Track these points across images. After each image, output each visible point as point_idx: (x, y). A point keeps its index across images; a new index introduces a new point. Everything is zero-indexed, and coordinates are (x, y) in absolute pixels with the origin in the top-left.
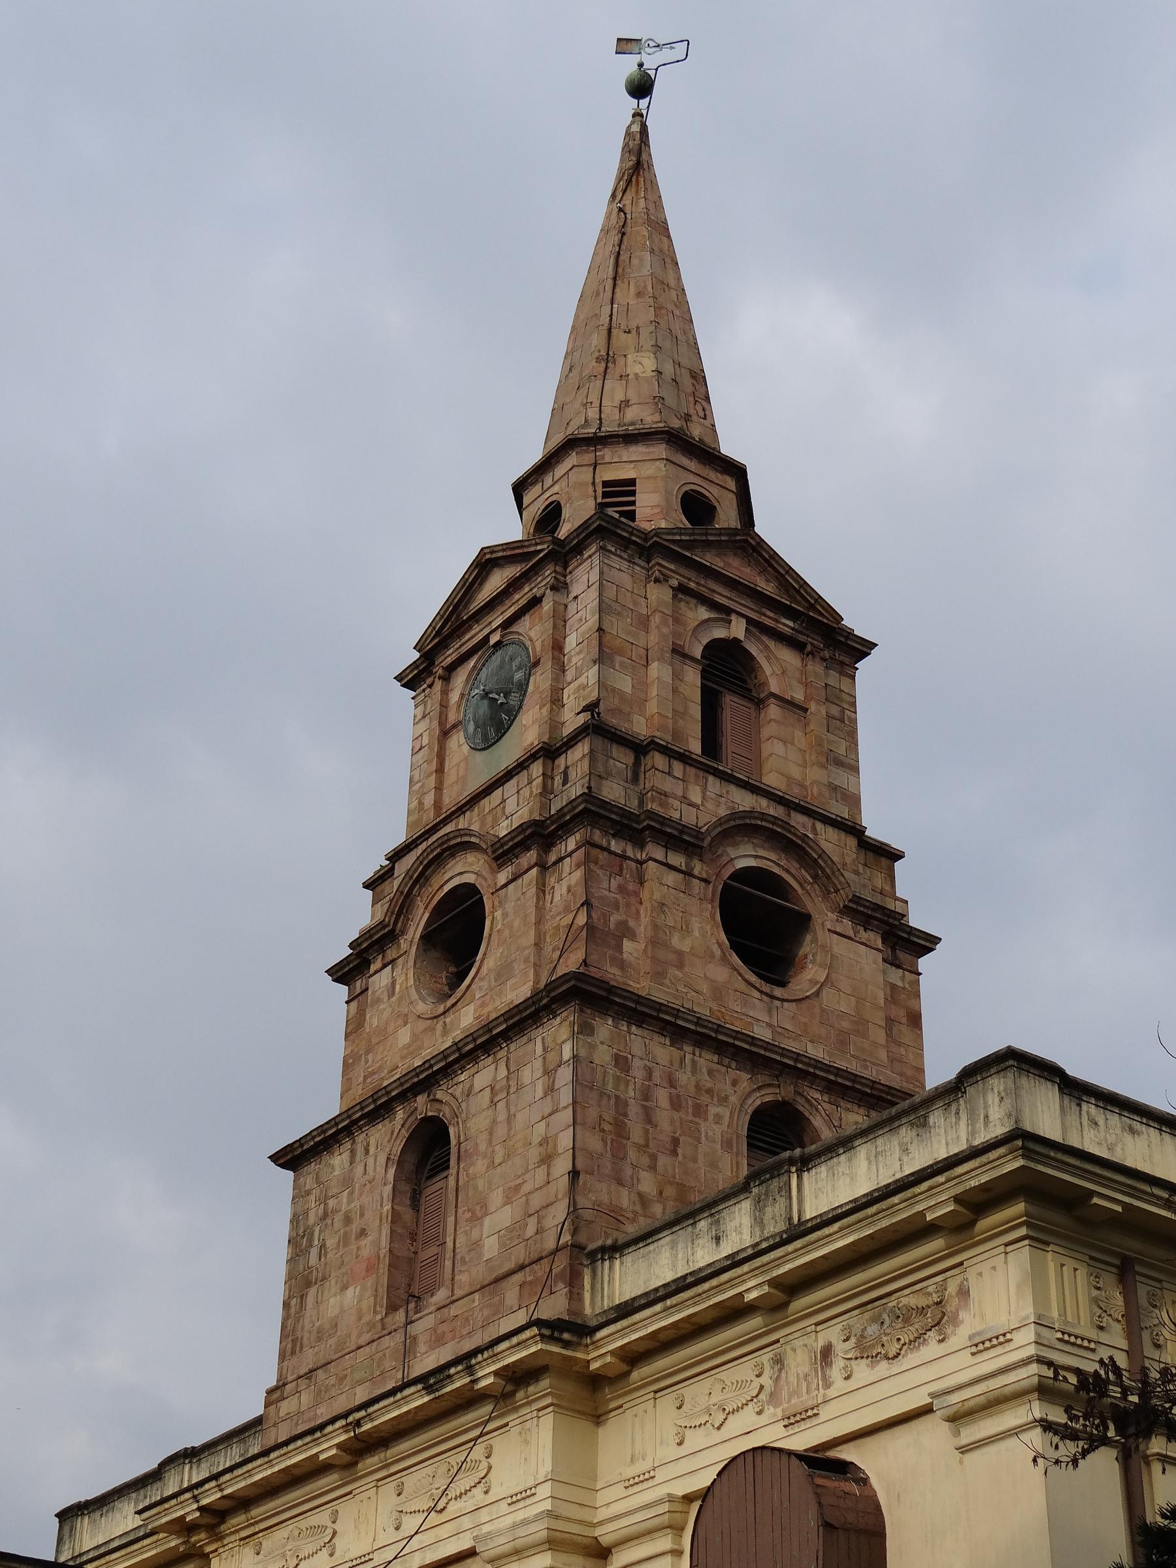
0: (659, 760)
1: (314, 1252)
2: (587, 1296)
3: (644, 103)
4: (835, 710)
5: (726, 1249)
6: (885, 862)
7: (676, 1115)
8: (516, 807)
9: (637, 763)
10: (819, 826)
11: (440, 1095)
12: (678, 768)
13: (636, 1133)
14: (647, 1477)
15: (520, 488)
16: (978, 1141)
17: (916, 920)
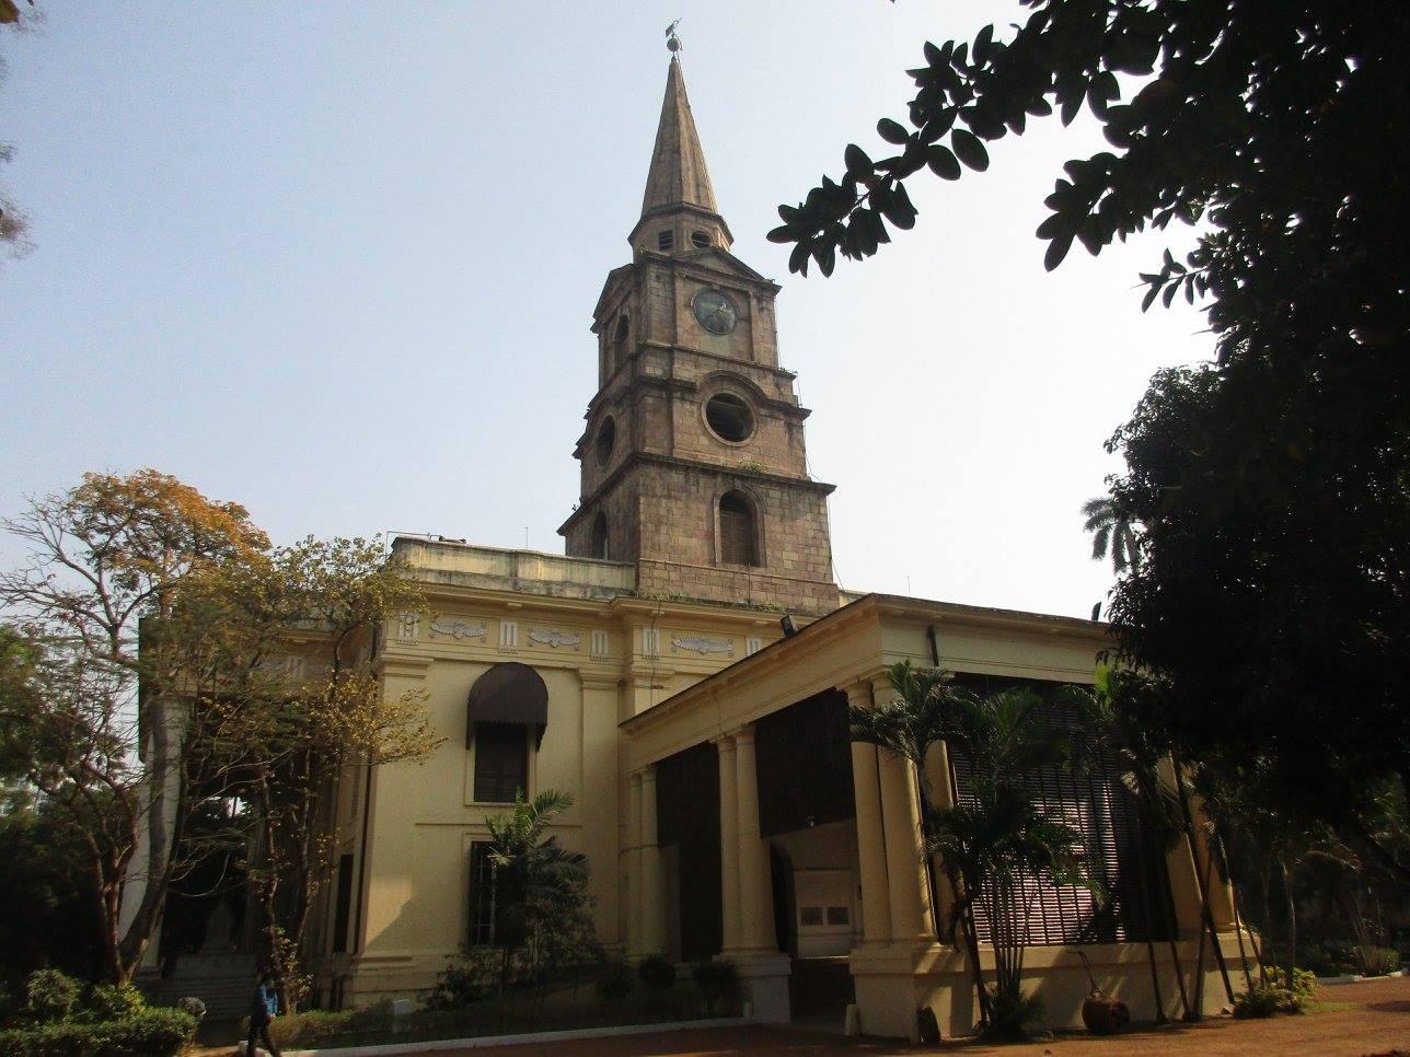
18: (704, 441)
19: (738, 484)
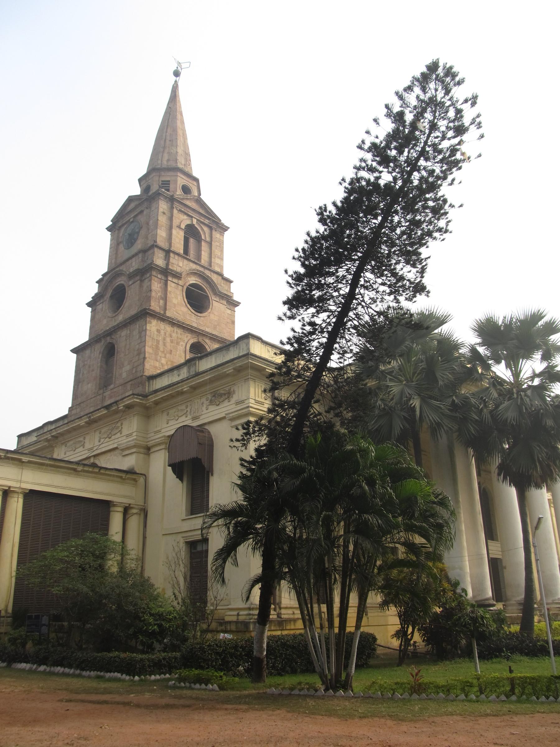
0: (172, 255)
1: (81, 375)
2: (147, 388)
3: (178, 78)
4: (218, 244)
5: (181, 378)
6: (228, 283)
7: (172, 344)
8: (135, 265)
9: (166, 255)
10: (212, 273)
11: (113, 337)
12: (176, 257)
13: (161, 347)
14: (159, 431)
15: (140, 180)
16: (241, 354)
17: (235, 298)
19: (108, 339)
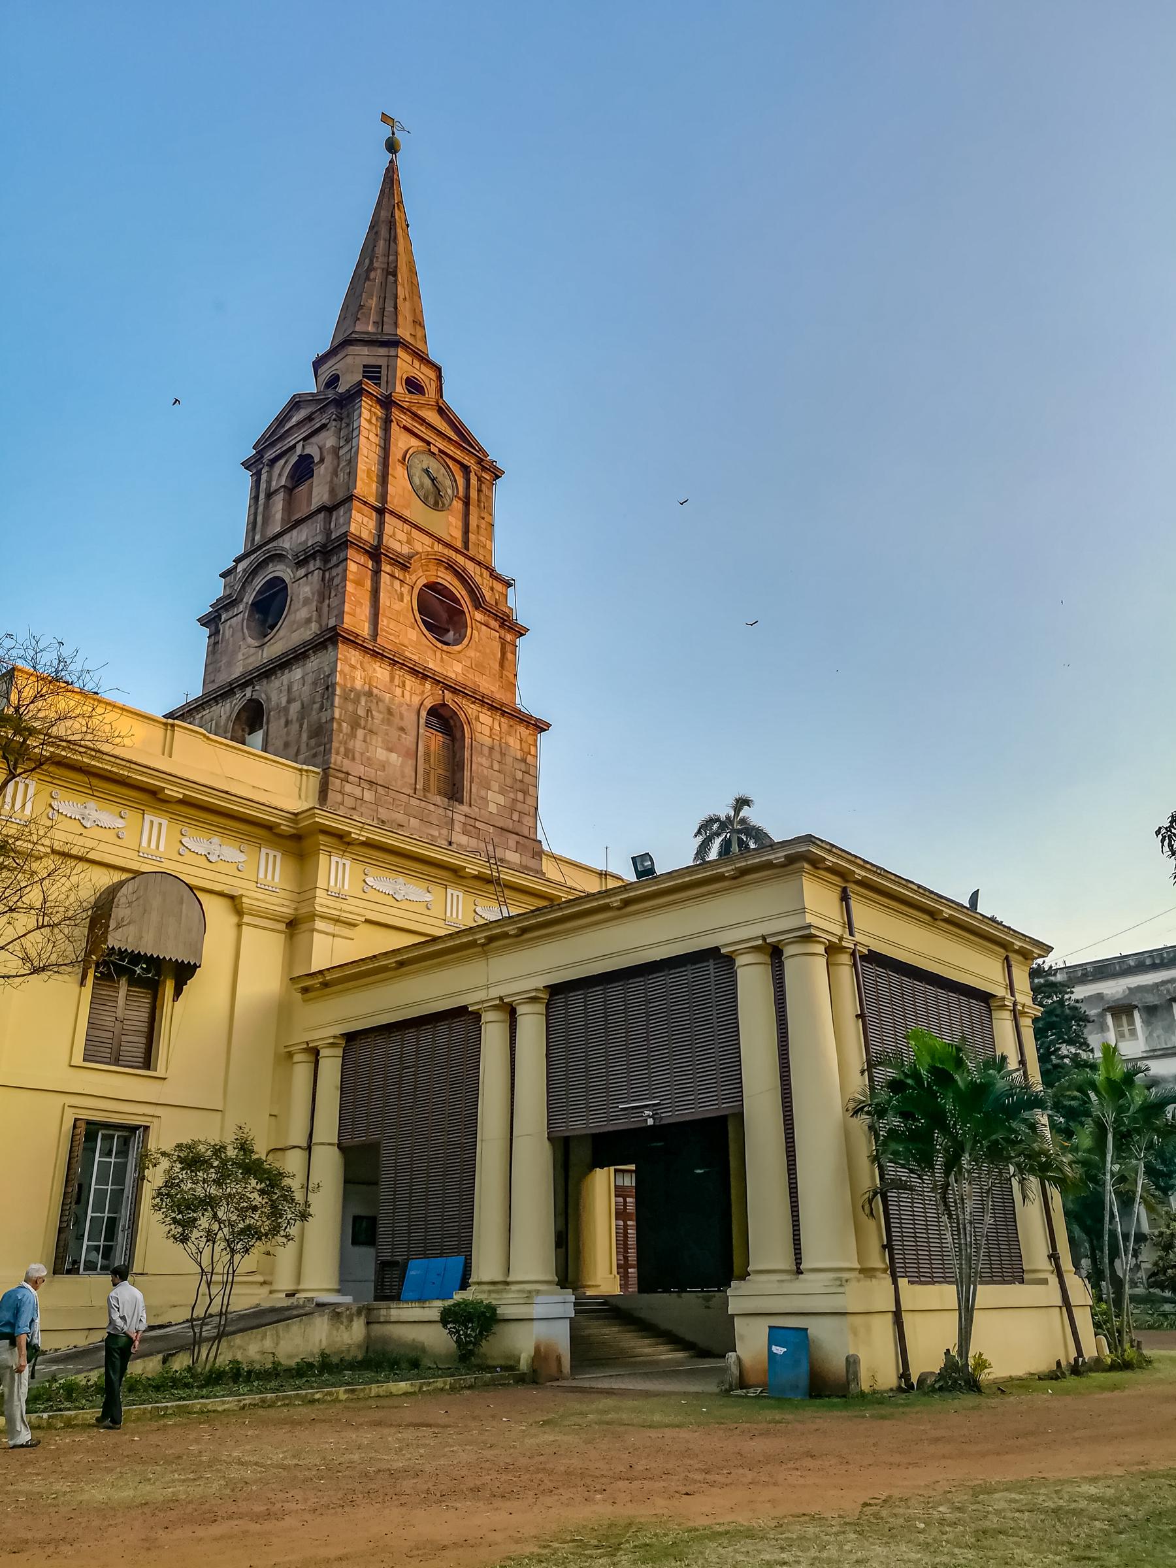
18: (413, 635)
